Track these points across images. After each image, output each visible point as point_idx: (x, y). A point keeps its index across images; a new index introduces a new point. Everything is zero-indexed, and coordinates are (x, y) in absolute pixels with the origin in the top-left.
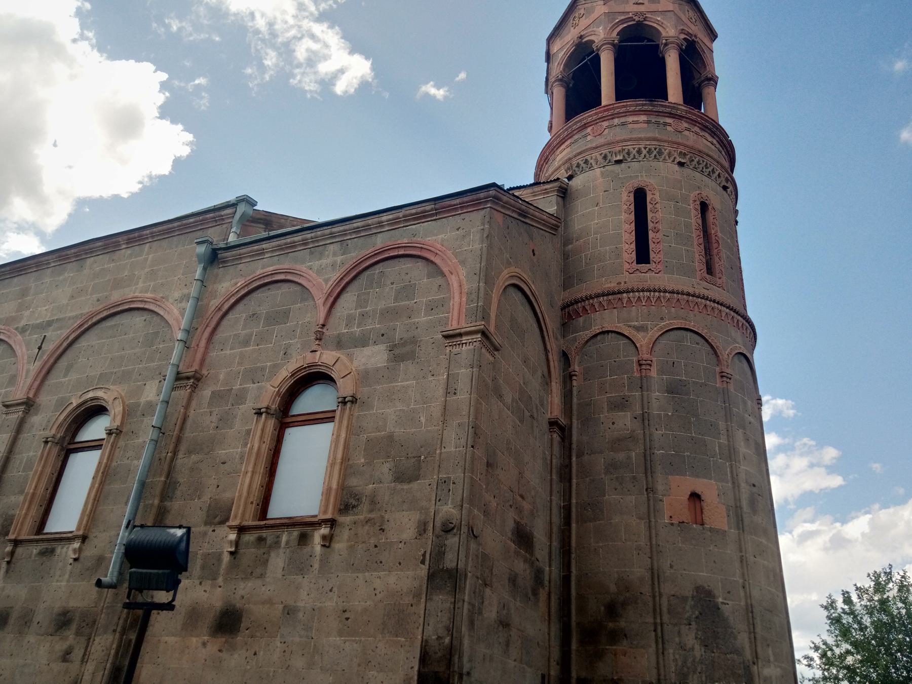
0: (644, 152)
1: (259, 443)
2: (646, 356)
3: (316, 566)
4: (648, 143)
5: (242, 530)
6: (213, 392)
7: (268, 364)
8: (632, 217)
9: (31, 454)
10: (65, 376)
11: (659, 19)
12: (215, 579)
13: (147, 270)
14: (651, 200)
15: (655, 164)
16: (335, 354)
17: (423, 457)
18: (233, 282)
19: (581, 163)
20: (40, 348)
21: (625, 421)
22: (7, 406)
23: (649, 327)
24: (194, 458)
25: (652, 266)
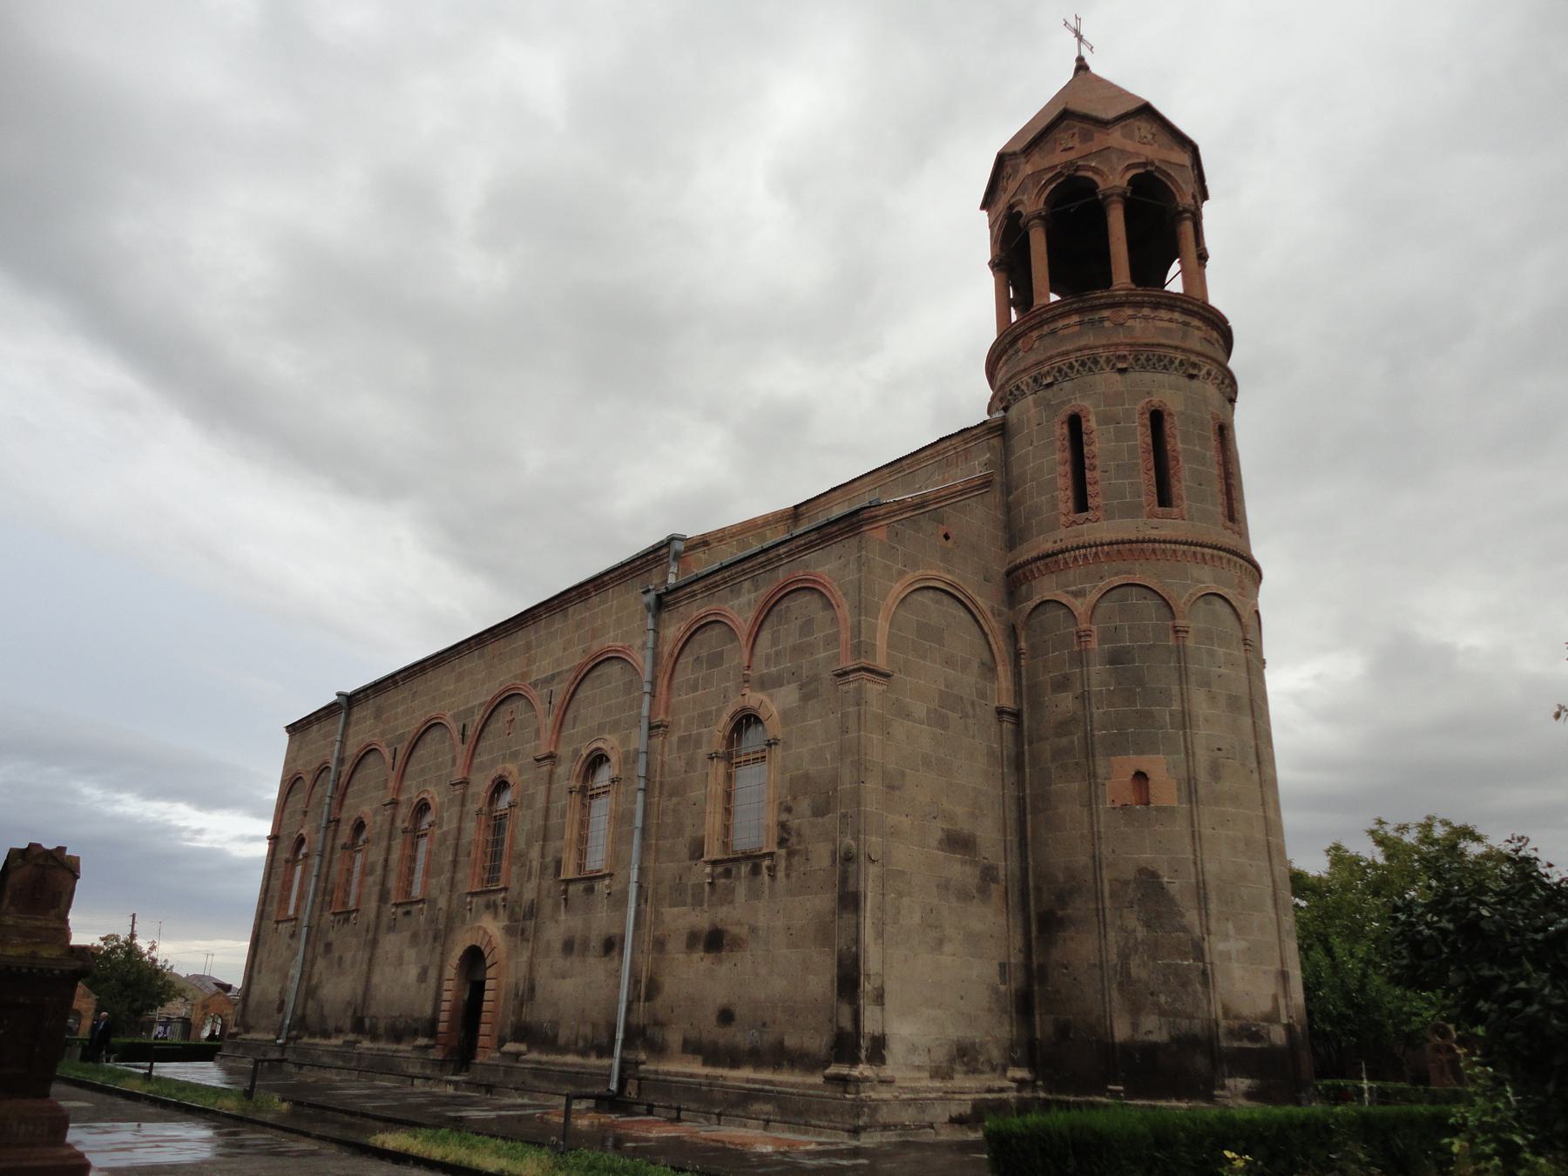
0: (1076, 364)
1: (716, 787)
2: (1084, 626)
3: (767, 891)
4: (1079, 354)
5: (714, 863)
6: (679, 738)
7: (714, 708)
8: (1067, 455)
9: (564, 802)
10: (574, 728)
11: (1093, 164)
12: (701, 905)
13: (614, 617)
14: (1086, 429)
15: (1089, 379)
16: (761, 696)
17: (830, 793)
18: (679, 625)
19: (1013, 389)
20: (550, 703)
21: (1065, 703)
22: (538, 760)
23: (1088, 589)
24: (675, 800)
25: (1091, 512)
